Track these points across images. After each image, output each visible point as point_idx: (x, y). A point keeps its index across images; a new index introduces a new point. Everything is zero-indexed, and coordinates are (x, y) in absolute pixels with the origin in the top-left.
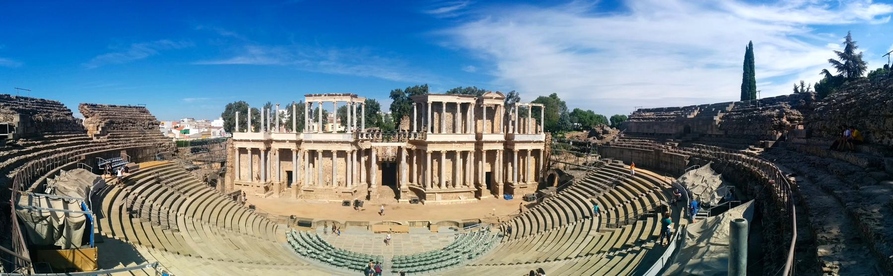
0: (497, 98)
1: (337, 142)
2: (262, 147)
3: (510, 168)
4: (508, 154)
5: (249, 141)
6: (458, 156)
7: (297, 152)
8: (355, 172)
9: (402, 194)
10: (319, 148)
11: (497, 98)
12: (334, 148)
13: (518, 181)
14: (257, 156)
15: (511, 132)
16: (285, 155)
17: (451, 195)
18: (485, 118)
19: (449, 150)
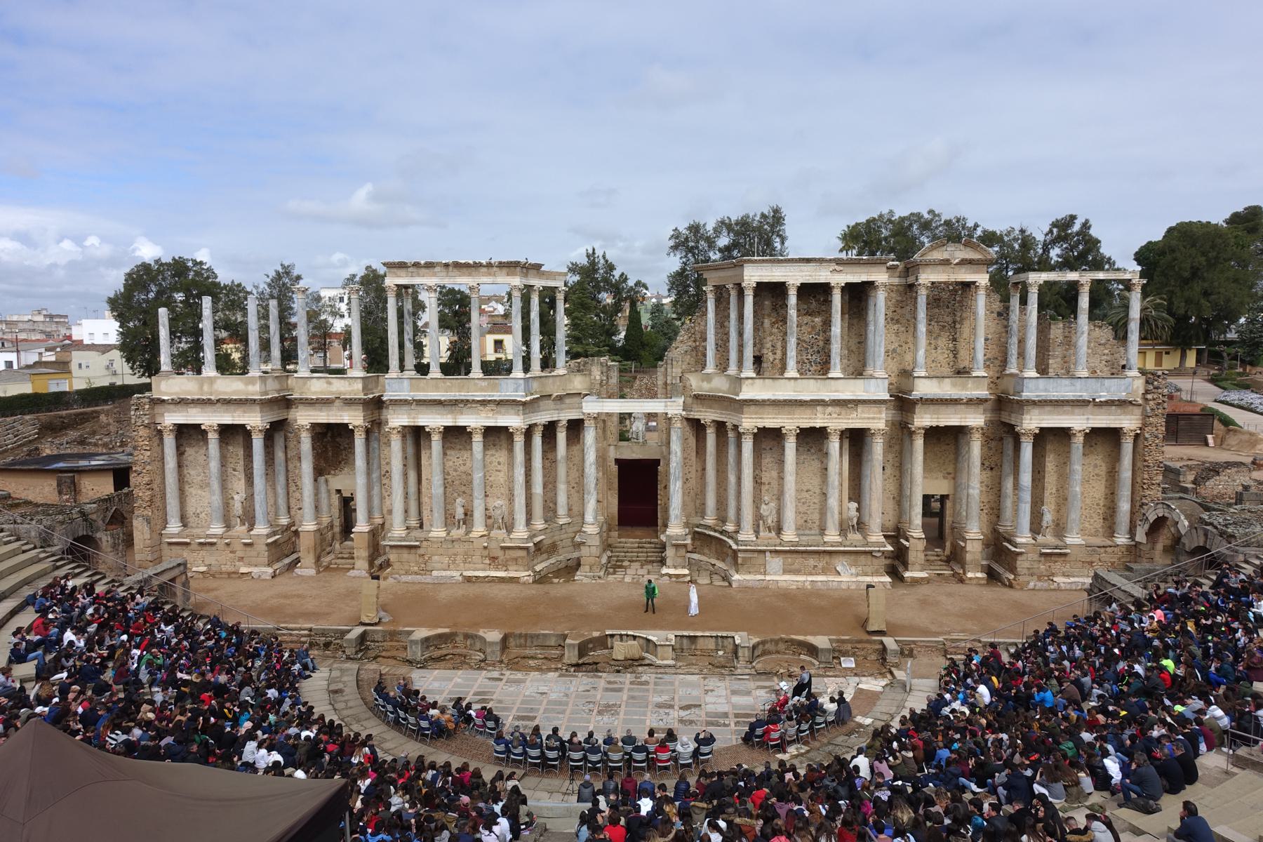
0: (964, 262)
1: (484, 403)
2: (255, 420)
3: (1009, 485)
5: (208, 402)
6: (834, 445)
7: (368, 432)
8: (538, 489)
9: (670, 552)
10: (434, 421)
11: (964, 262)
12: (474, 420)
13: (1036, 529)
14: (237, 451)
15: (1013, 369)
16: (332, 443)
17: (812, 561)
18: (922, 328)
19: (806, 424)
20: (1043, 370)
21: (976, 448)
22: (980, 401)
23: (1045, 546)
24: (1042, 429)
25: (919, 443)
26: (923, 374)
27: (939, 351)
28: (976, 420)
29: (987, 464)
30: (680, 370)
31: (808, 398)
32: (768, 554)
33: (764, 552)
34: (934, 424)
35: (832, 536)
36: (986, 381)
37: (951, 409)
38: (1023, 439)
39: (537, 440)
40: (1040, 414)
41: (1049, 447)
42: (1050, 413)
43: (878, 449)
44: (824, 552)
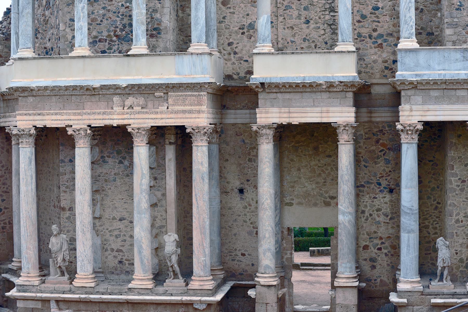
4: (378, 142)
6: (141, 152)
19: (100, 121)
20: (429, 37)
21: (345, 154)
22: (345, 86)
23: (437, 295)
24: (426, 124)
25: (266, 150)
26: (266, 50)
27: (312, 25)
28: (342, 114)
29: (384, 183)
31: (97, 85)
32: (53, 305)
33: (46, 301)
34: (285, 121)
35: (141, 278)
36: (353, 59)
37: (308, 97)
38: (404, 138)
40: (424, 103)
41: (451, 153)
42: (437, 101)
43: (201, 154)
44: (128, 303)
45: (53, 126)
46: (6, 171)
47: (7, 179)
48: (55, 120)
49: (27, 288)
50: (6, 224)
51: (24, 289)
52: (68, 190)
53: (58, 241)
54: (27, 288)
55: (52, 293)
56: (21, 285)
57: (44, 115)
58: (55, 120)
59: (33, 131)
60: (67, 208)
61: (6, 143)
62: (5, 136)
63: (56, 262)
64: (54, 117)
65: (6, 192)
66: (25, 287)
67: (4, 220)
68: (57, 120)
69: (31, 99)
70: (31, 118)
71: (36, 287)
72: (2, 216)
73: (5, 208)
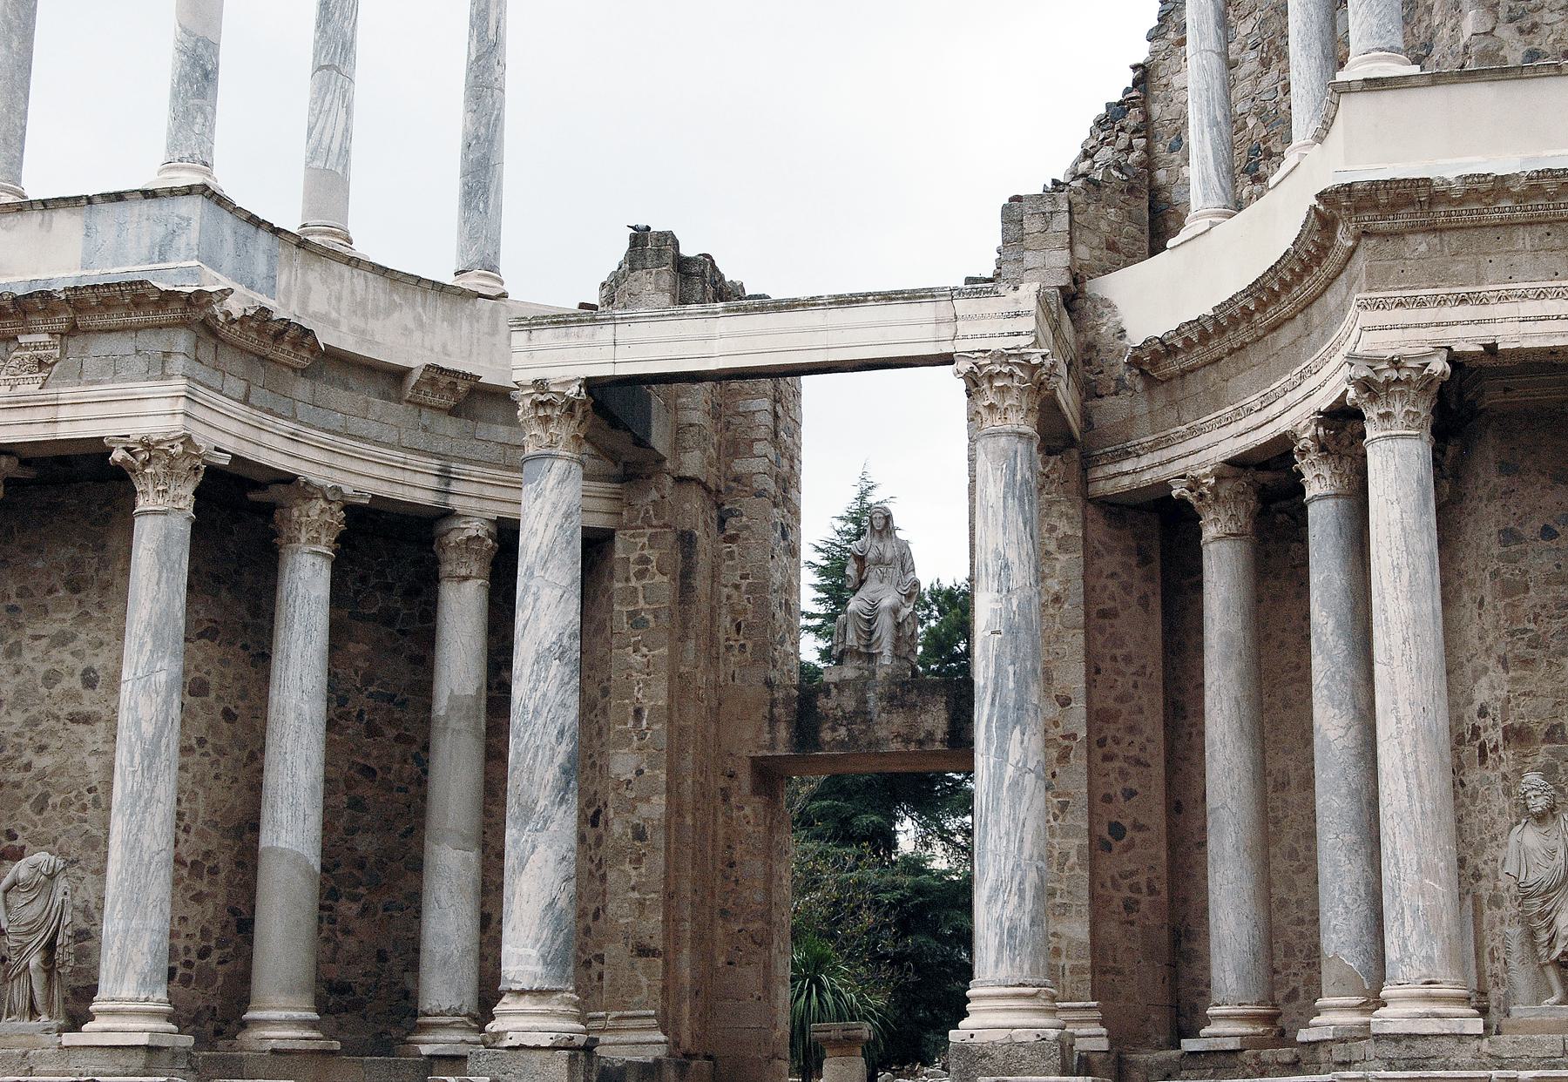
30: (1060, 258)
39: (307, 583)
45: (1527, 344)
46: (1140, 680)
47: (1141, 711)
48: (1539, 319)
49: (1431, 1048)
50: (1139, 891)
51: (1414, 1053)
52: (1538, 653)
53: (1552, 843)
54: (1431, 1048)
55: (1555, 1066)
56: (1396, 1038)
57: (1483, 301)
58: (1539, 319)
59: (1439, 365)
60: (1540, 730)
61: (1138, 572)
62: (1133, 544)
63: (1544, 936)
64: (1531, 308)
65: (1138, 762)
66: (1418, 1044)
67: (1132, 874)
68: (1547, 318)
69: (1421, 244)
70: (1427, 315)
71: (1475, 1044)
72: (1125, 857)
73: (1139, 827)
